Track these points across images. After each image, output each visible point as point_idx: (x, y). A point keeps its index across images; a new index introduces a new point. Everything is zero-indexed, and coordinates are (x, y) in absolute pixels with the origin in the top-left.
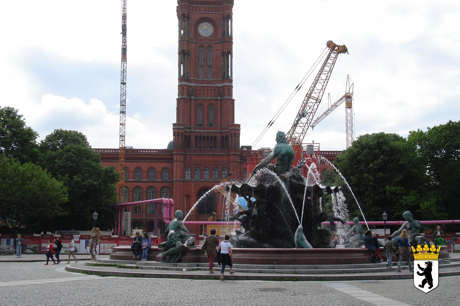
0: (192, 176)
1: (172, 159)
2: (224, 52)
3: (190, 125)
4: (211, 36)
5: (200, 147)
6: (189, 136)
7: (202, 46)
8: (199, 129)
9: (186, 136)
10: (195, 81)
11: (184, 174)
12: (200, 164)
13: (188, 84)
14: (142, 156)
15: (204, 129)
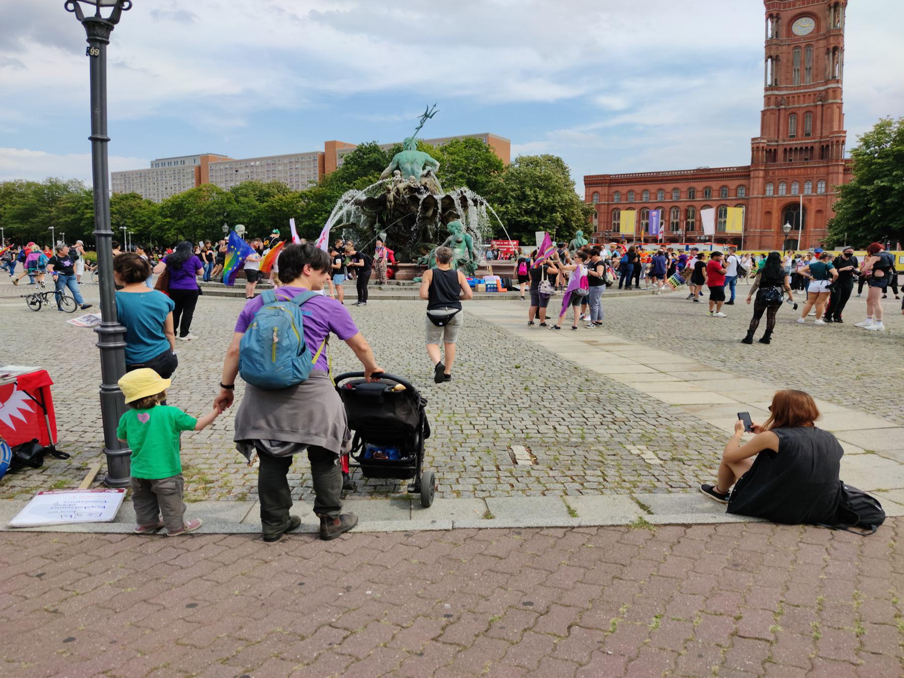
0: (776, 191)
1: (749, 175)
2: (828, 49)
3: (778, 137)
4: (812, 32)
5: (791, 160)
6: (775, 150)
7: (797, 47)
8: (790, 141)
9: (770, 150)
10: (787, 88)
11: (765, 191)
12: (787, 179)
13: (776, 92)
14: (712, 175)
15: (796, 140)
